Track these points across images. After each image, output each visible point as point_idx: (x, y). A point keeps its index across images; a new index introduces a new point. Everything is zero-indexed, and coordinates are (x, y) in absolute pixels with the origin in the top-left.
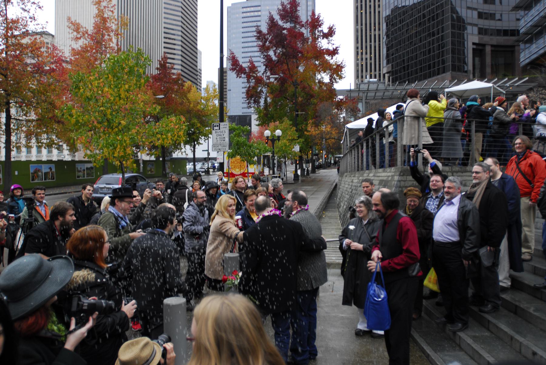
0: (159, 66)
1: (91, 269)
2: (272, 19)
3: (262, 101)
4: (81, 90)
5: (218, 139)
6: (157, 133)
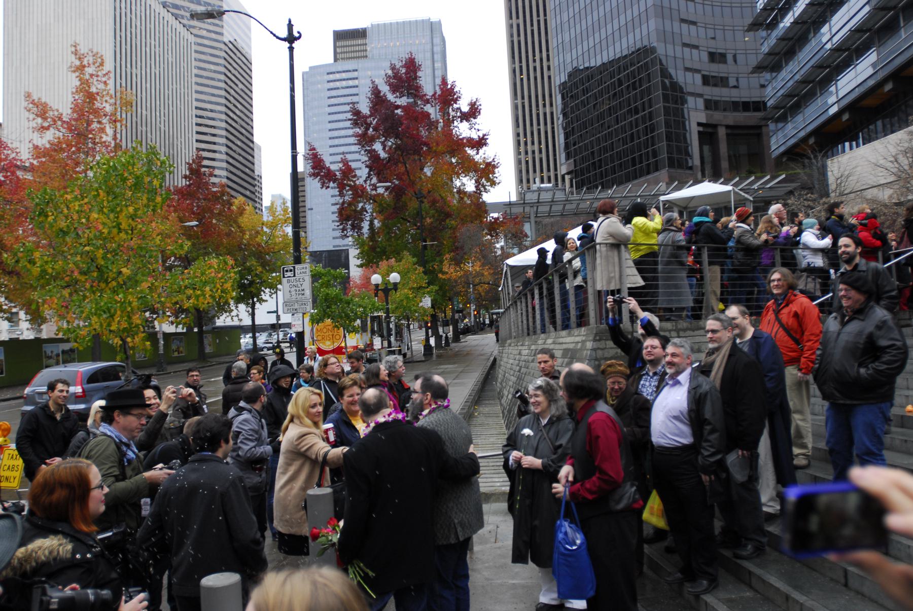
0: (188, 173)
1: (65, 535)
2: (376, 92)
3: (366, 226)
4: (50, 219)
5: (293, 293)
6: (186, 287)
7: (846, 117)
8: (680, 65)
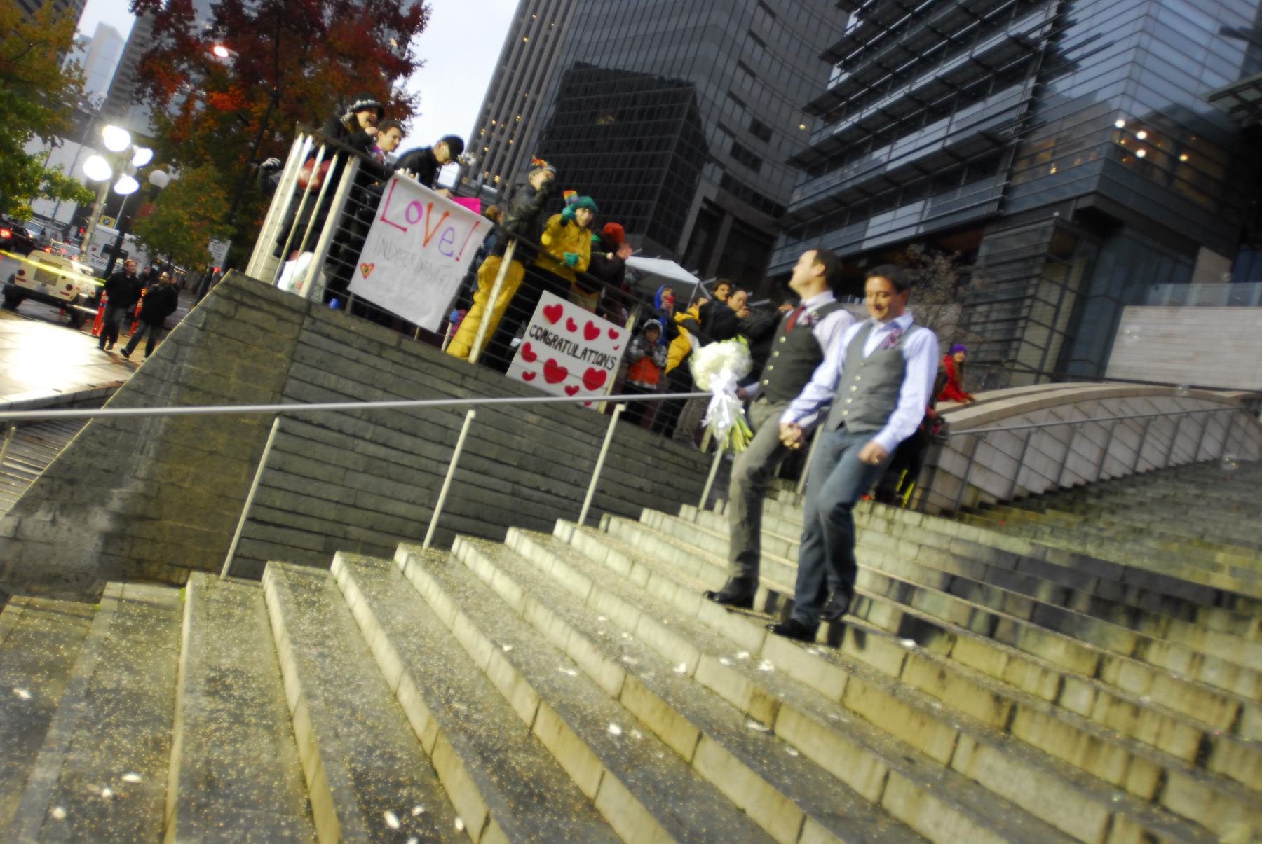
3: (177, 98)
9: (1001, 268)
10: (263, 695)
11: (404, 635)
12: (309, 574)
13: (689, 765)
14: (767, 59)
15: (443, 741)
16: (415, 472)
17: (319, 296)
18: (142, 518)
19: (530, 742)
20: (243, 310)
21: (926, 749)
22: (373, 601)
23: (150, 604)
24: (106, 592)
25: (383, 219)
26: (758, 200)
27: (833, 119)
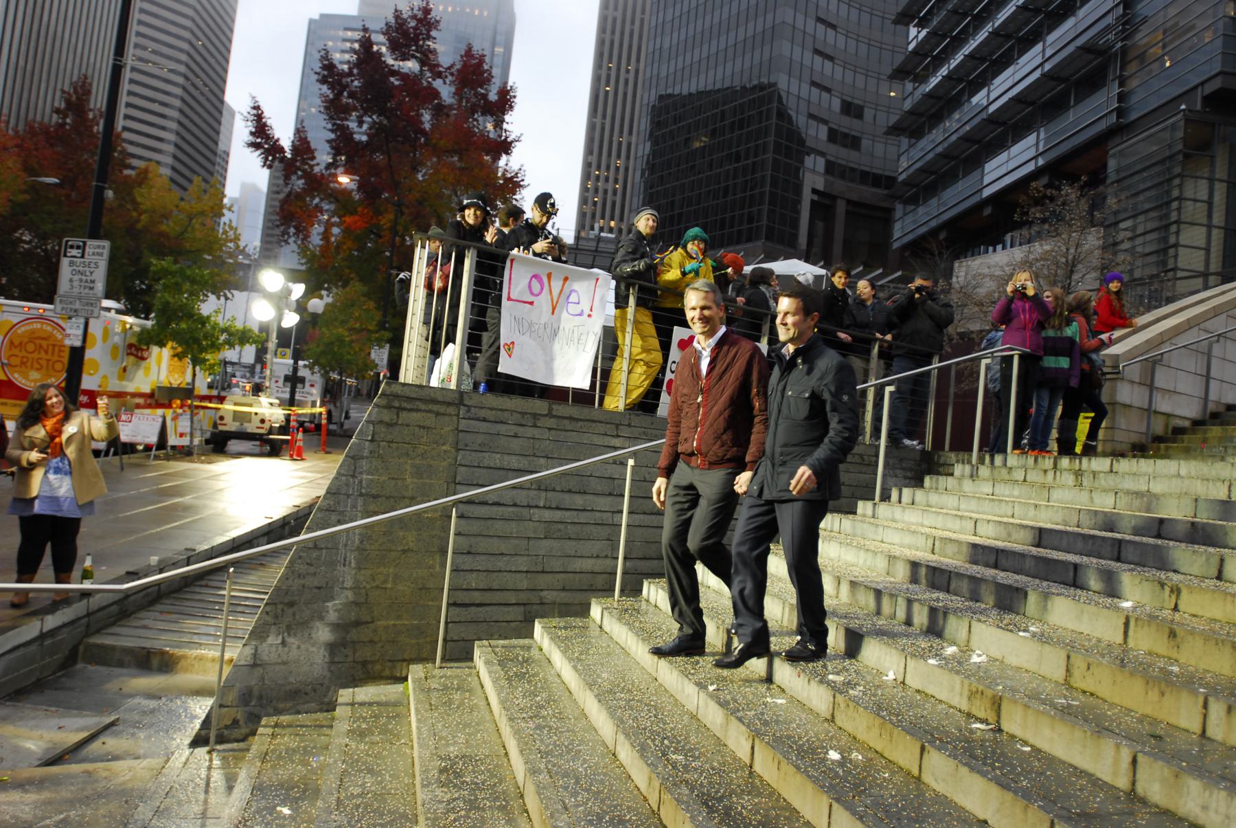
0: (63, 106)
2: (366, 44)
3: (316, 231)
5: (76, 284)
7: (988, 211)
8: (803, 105)
9: (1137, 178)
10: (492, 776)
11: (610, 691)
12: (515, 647)
13: (919, 779)
14: (841, 39)
15: (667, 797)
16: (592, 527)
17: (467, 385)
18: (358, 624)
19: (753, 783)
20: (404, 415)
21: (1173, 721)
22: (577, 662)
23: (379, 704)
24: (340, 700)
25: (509, 299)
26: (867, 177)
27: (922, 79)
